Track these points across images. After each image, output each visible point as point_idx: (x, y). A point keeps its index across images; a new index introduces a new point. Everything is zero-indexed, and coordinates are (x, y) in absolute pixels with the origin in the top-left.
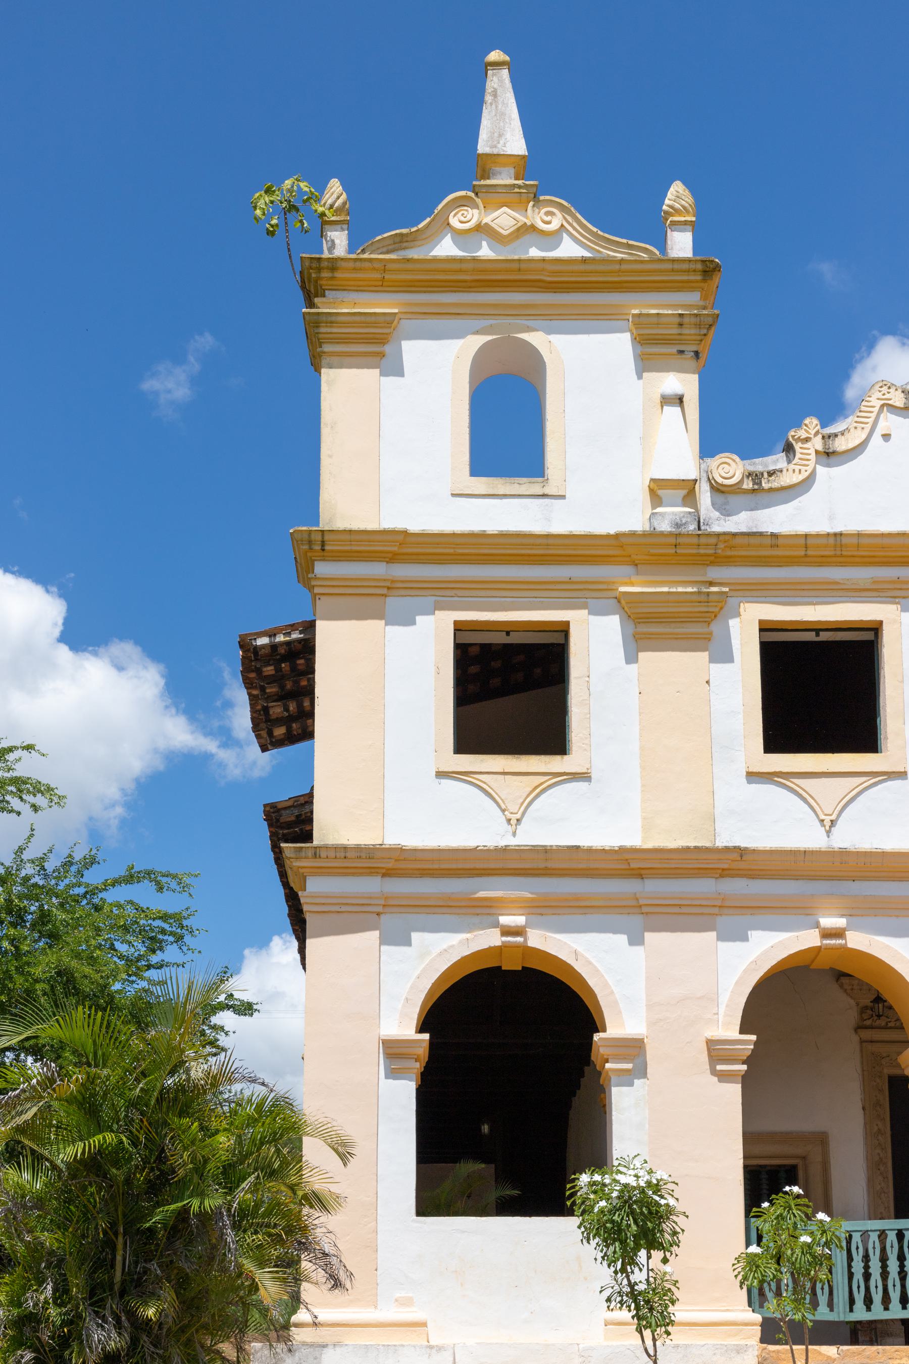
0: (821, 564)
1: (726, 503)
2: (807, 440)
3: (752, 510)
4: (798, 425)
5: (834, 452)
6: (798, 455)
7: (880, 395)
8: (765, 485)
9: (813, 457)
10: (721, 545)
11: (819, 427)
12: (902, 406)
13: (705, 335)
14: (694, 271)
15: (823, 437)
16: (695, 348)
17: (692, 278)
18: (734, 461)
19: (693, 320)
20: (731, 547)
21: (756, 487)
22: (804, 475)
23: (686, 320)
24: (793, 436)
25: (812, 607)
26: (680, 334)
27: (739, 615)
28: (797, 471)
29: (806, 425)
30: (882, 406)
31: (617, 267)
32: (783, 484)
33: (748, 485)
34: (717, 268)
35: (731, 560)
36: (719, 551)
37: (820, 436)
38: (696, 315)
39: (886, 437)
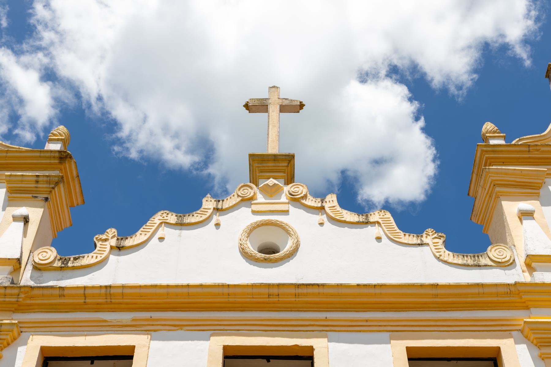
0: (97, 310)
1: (40, 277)
2: (106, 240)
3: (58, 280)
4: (103, 233)
5: (123, 247)
6: (98, 248)
7: (161, 218)
8: (70, 264)
9: (108, 249)
10: (22, 296)
11: (116, 233)
12: (174, 223)
13: (53, 188)
14: (54, 157)
15: (118, 239)
16: (46, 196)
17: (52, 161)
18: (51, 250)
19: (45, 179)
20: (31, 297)
21: (63, 265)
22: (99, 259)
23: (40, 179)
24: (97, 238)
25: (84, 337)
26: (36, 187)
27: (25, 344)
28: (95, 257)
29: (107, 233)
30: (161, 223)
31: (5, 154)
32: (83, 264)
33: (58, 264)
34: (70, 157)
35: (31, 307)
36: (21, 300)
37: (116, 238)
38: (48, 176)
39: (161, 239)
